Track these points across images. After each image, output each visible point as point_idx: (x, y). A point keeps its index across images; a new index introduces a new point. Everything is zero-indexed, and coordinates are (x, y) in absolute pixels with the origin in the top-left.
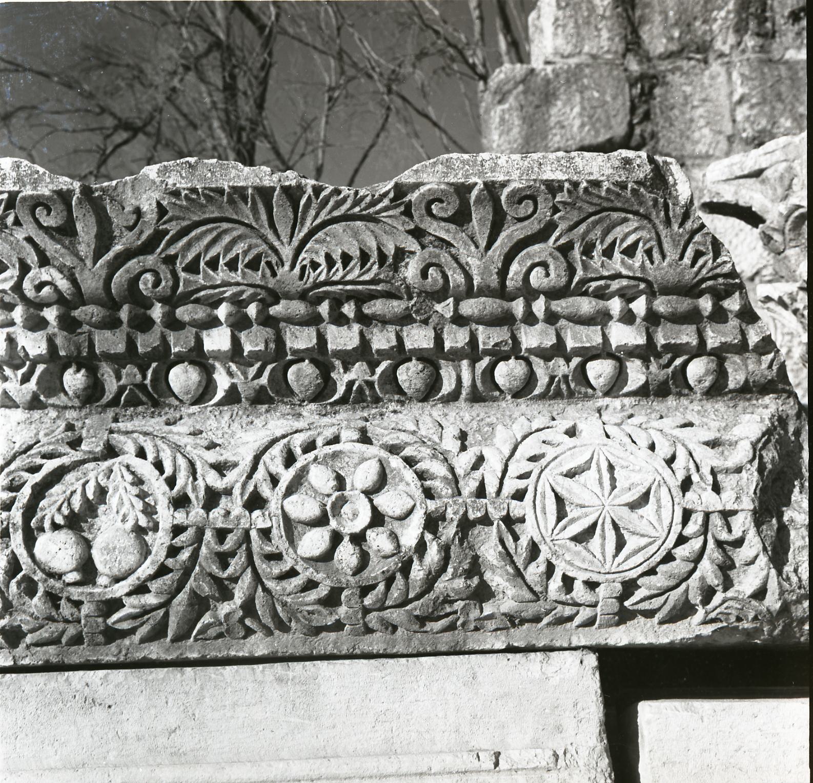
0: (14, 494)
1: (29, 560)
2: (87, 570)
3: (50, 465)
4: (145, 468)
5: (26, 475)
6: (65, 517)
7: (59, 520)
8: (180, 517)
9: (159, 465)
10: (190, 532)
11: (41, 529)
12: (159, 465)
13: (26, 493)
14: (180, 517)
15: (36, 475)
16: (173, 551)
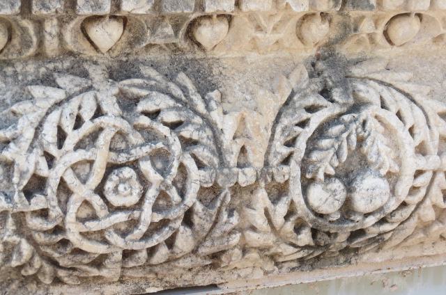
0: (291, 149)
1: (305, 206)
2: (347, 209)
3: (316, 120)
4: (393, 121)
5: (299, 129)
6: (336, 169)
7: (332, 171)
8: (421, 163)
9: (399, 114)
10: (428, 175)
11: (313, 180)
12: (399, 114)
13: (301, 145)
14: (421, 163)
15: (307, 129)
16: (413, 190)
